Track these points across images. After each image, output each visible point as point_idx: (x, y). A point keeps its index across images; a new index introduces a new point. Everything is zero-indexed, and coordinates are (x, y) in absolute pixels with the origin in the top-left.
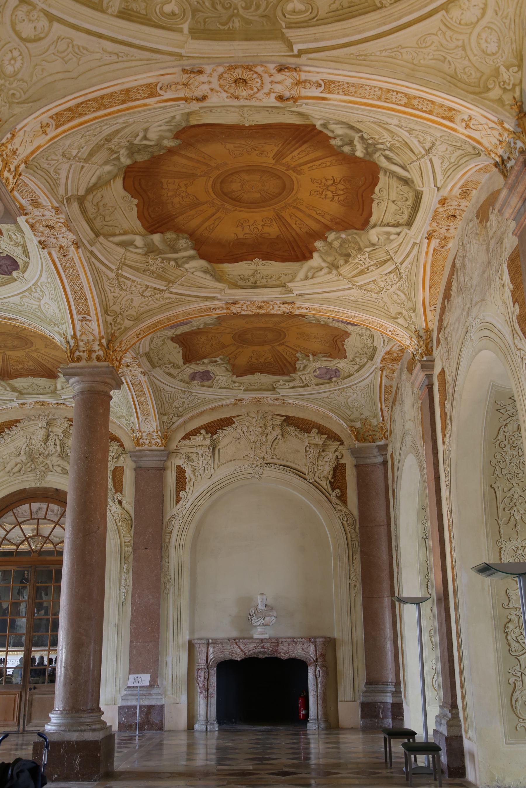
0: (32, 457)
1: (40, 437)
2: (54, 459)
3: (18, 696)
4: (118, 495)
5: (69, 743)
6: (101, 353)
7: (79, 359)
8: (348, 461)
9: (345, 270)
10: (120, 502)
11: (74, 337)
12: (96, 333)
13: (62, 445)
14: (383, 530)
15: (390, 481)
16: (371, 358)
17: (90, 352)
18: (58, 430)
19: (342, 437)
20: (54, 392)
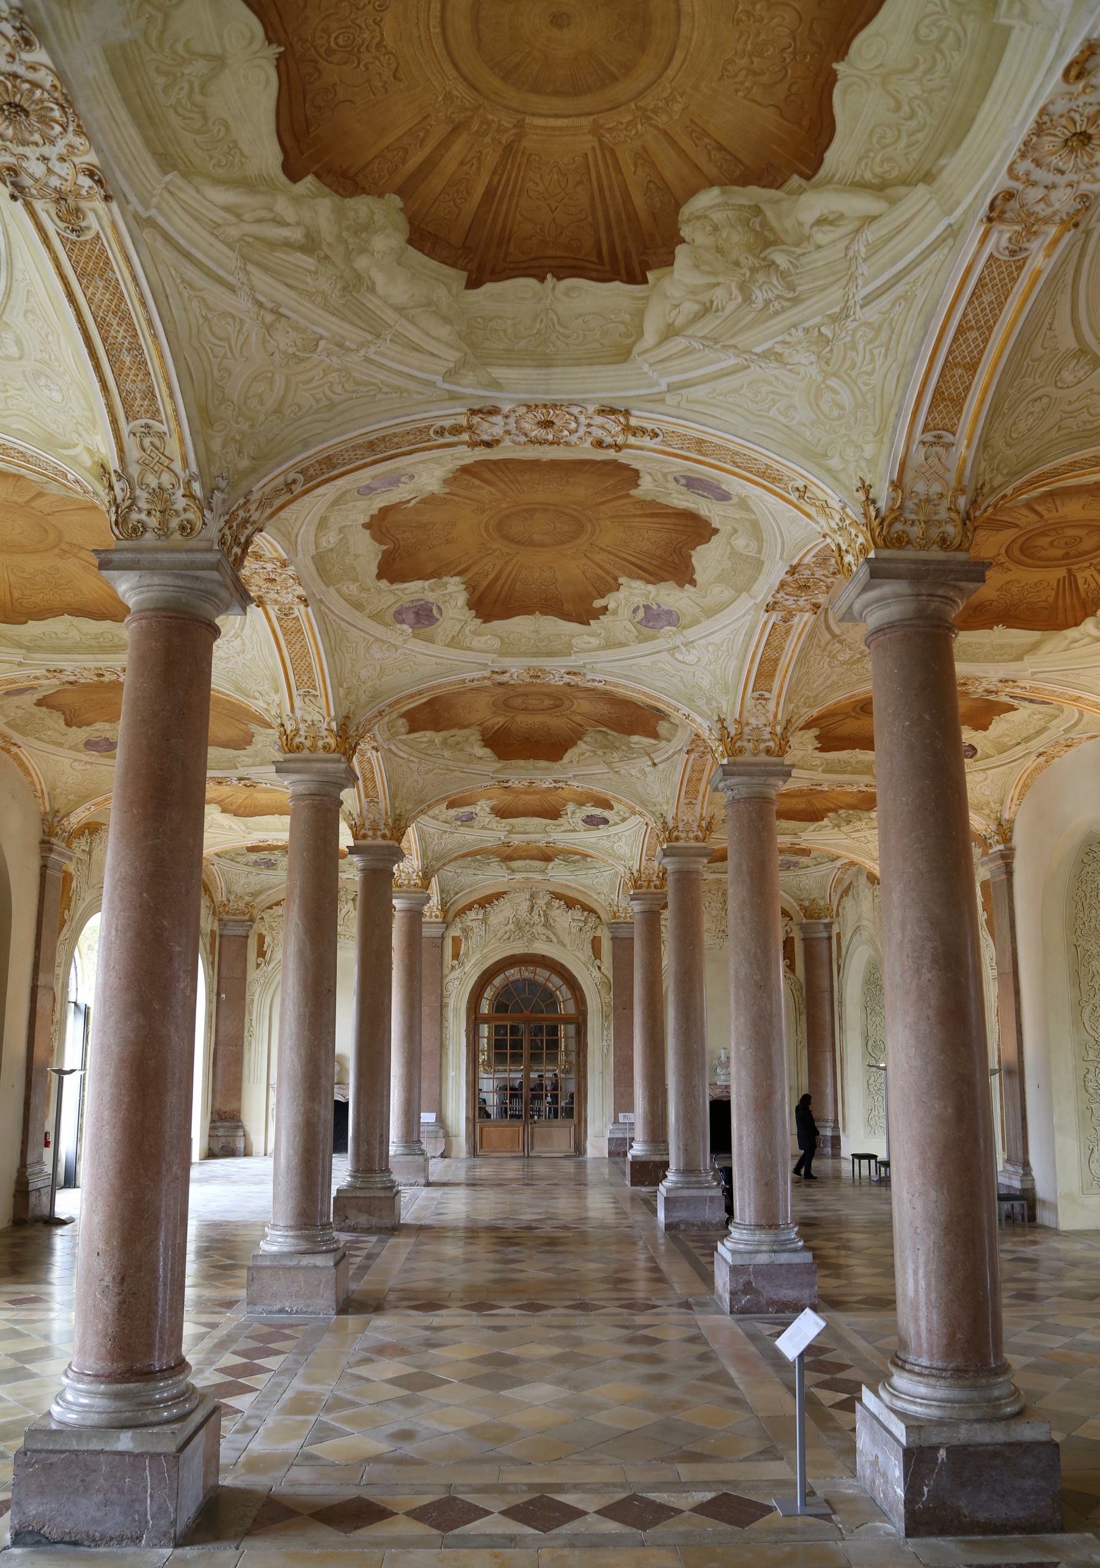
0: (519, 926)
1: (525, 908)
2: (540, 929)
3: (521, 1129)
4: (598, 962)
5: (654, 1162)
6: (658, 883)
7: (641, 887)
8: (797, 935)
9: (845, 829)
10: (599, 968)
11: (639, 871)
12: (656, 869)
13: (546, 915)
14: (827, 995)
15: (834, 955)
16: (833, 861)
17: (650, 881)
18: (541, 902)
19: (791, 913)
20: (543, 871)
